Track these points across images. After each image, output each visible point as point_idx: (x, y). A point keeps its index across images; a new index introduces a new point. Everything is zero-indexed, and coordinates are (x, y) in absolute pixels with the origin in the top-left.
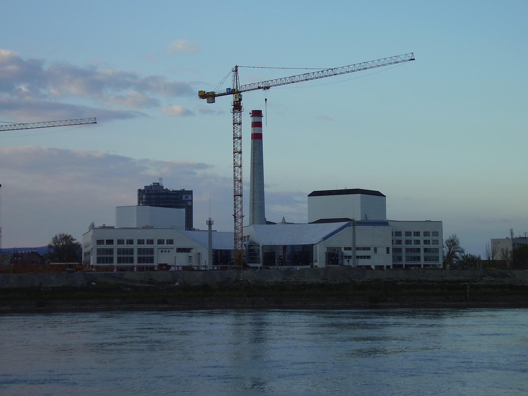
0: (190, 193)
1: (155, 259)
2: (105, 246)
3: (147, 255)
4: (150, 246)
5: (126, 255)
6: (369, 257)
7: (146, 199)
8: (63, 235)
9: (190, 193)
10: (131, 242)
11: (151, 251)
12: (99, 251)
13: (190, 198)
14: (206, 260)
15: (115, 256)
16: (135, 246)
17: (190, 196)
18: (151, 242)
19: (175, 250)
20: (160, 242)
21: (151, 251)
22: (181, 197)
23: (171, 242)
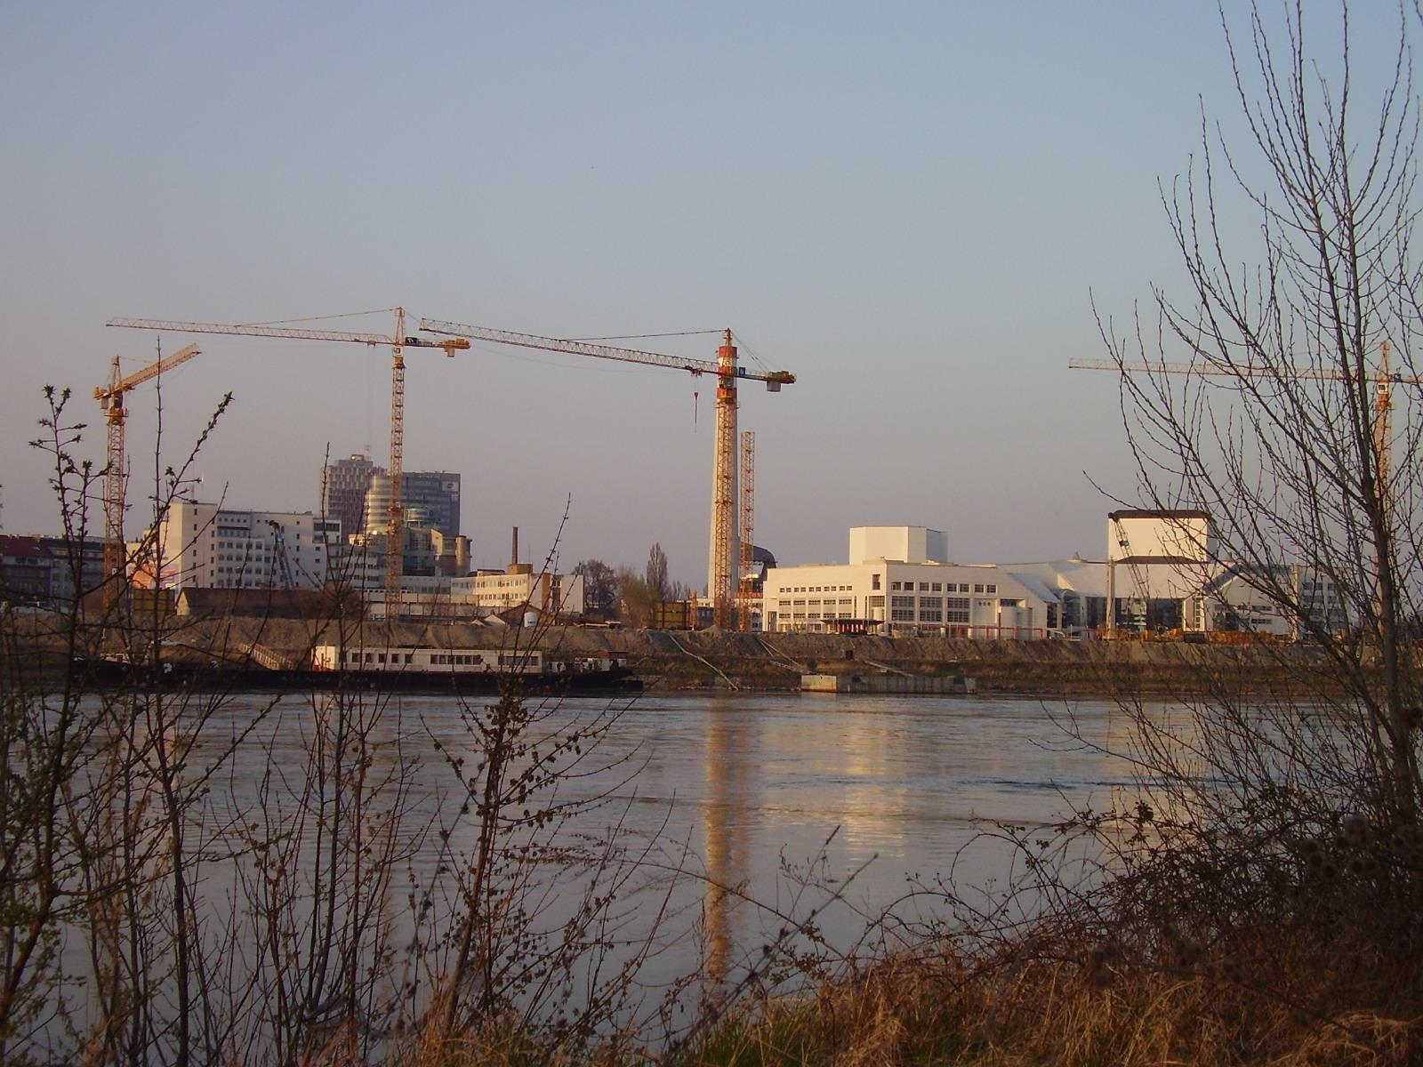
0: (457, 477)
1: (971, 616)
2: (902, 592)
3: (960, 611)
4: (964, 595)
5: (931, 610)
6: (1269, 622)
7: (377, 487)
8: (594, 561)
9: (457, 477)
10: (937, 587)
11: (966, 603)
12: (894, 600)
13: (455, 488)
14: (1040, 621)
15: (917, 608)
16: (943, 594)
17: (455, 484)
18: (965, 588)
19: (997, 602)
20: (978, 589)
21: (966, 603)
22: (440, 485)
23: (992, 589)
